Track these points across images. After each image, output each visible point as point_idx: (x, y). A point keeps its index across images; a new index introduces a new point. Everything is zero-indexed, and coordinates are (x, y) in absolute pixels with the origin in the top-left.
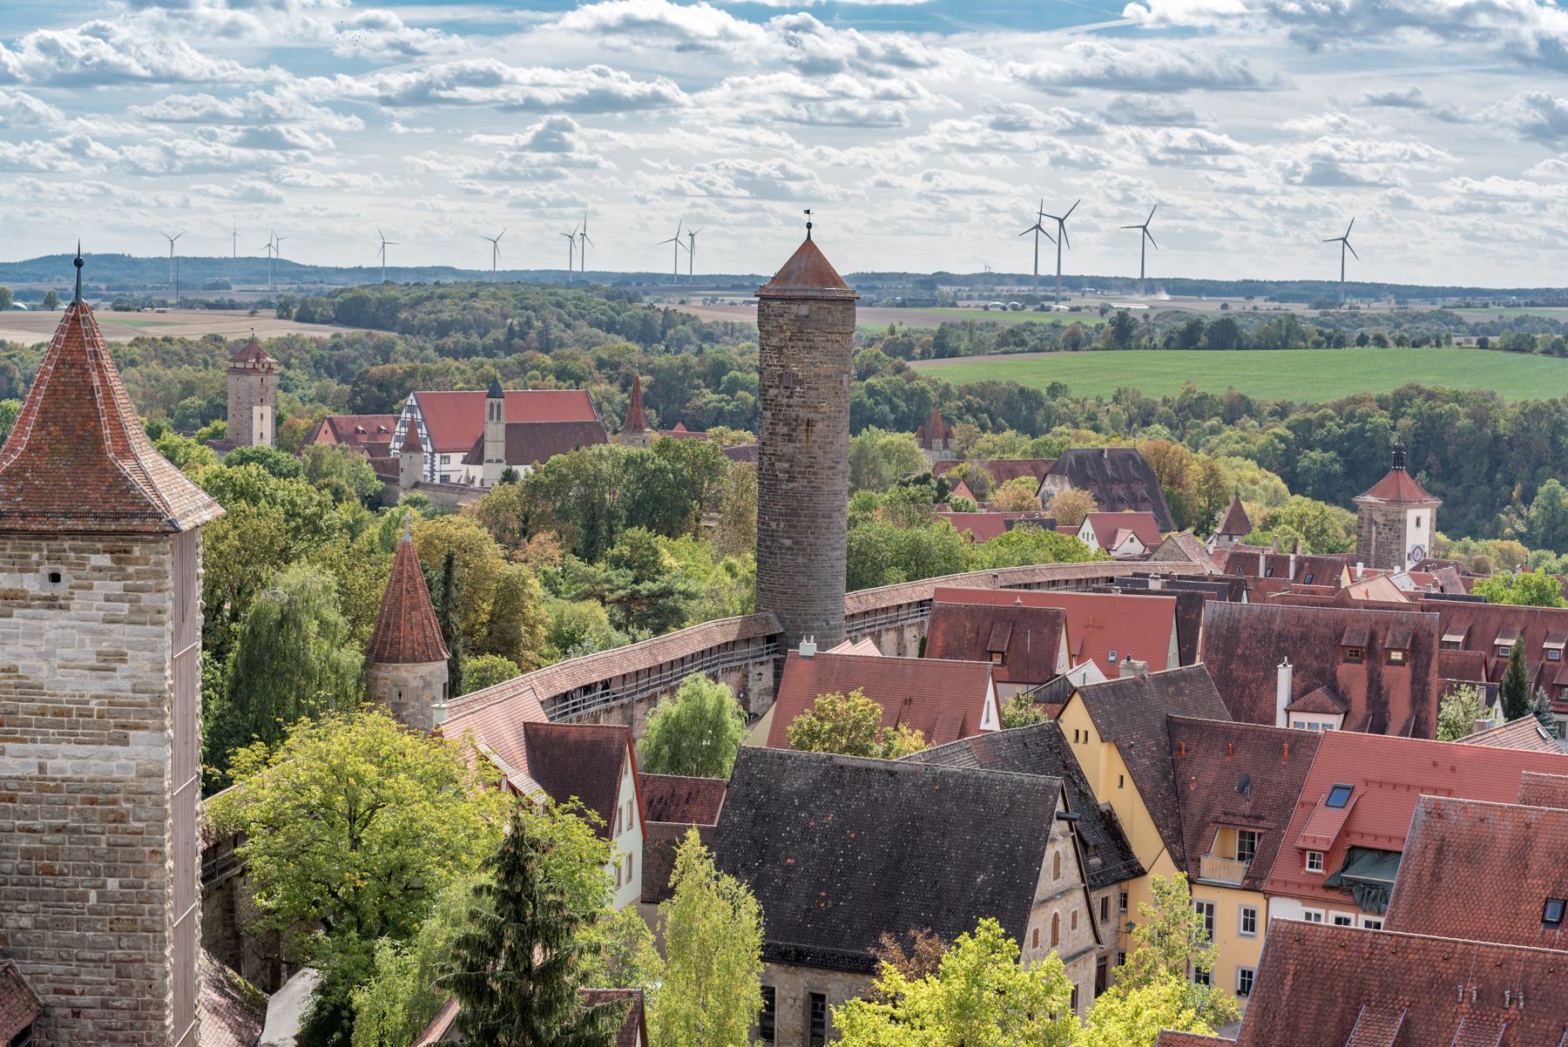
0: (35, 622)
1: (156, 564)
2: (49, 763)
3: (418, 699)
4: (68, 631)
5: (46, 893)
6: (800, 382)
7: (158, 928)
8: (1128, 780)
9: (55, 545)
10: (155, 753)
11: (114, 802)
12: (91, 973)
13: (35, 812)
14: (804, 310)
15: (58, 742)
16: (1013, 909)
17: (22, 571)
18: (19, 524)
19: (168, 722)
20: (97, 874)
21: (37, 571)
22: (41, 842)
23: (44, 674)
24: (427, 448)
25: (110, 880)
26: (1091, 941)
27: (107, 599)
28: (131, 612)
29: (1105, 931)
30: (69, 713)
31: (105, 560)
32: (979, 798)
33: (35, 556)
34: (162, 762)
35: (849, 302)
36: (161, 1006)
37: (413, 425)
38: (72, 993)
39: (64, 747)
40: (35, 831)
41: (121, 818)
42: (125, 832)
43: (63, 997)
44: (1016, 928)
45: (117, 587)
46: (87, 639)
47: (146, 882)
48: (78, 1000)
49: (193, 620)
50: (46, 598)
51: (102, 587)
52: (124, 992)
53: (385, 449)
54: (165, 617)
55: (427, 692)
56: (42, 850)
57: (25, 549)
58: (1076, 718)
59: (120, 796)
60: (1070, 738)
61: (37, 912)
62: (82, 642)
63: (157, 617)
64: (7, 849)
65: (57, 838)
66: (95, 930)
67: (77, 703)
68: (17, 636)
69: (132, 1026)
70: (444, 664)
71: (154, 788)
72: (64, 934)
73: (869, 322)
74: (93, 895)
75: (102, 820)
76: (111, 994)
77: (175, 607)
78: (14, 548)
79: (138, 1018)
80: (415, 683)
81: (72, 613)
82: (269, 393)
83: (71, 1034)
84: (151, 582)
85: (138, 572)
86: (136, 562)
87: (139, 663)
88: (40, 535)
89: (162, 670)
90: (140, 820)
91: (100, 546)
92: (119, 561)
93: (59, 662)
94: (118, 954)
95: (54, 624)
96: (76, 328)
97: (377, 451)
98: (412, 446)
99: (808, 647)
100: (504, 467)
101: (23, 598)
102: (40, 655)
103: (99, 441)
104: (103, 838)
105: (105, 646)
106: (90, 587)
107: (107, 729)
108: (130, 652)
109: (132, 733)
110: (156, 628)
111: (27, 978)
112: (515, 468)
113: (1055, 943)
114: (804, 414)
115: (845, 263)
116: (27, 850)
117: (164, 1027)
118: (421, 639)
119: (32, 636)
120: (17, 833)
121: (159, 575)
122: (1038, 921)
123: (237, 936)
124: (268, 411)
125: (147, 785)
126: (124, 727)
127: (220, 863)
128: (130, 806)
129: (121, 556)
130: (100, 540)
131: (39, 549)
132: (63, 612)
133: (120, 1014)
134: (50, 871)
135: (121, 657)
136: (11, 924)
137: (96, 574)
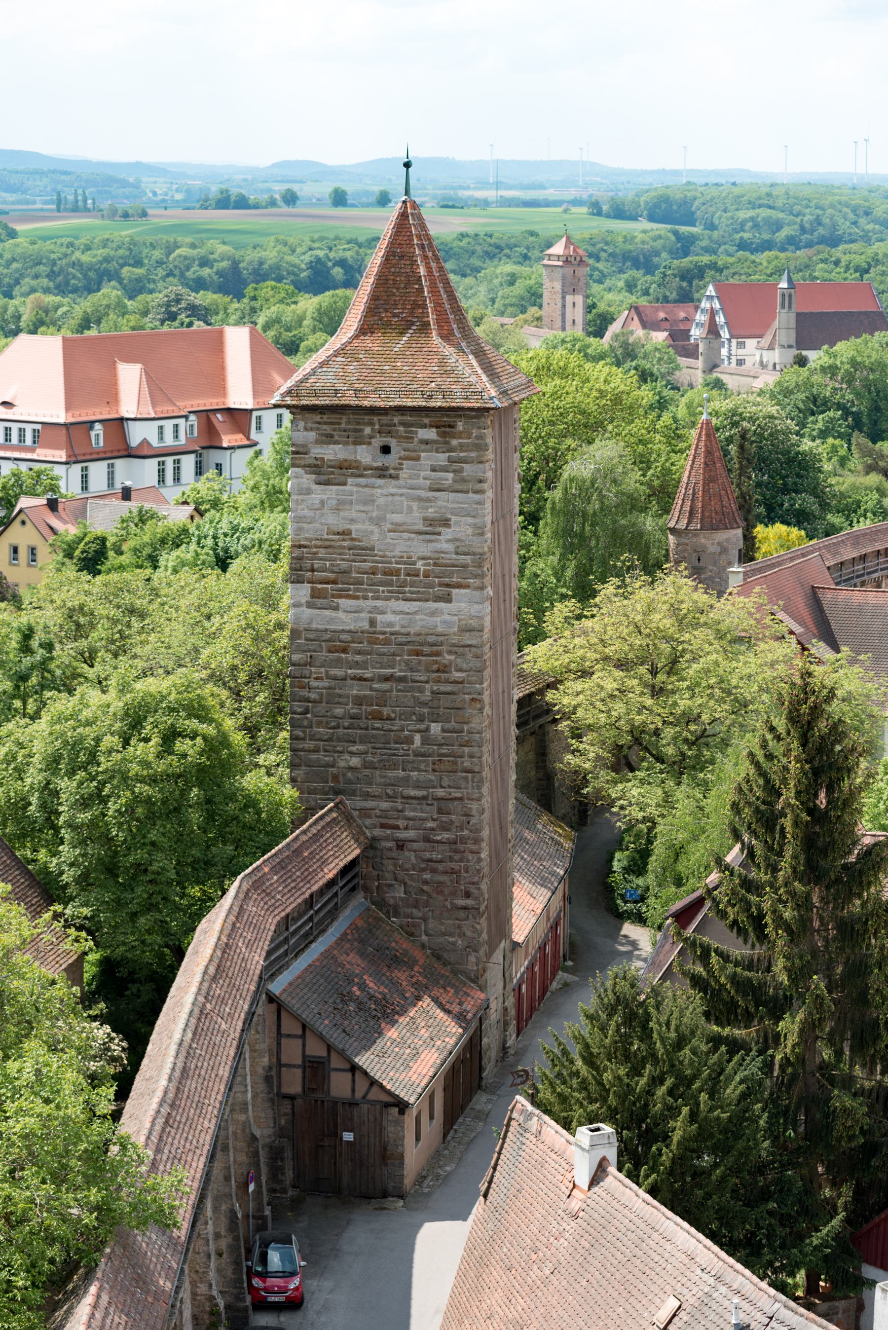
0: (367, 490)
1: (477, 437)
2: (379, 618)
3: (715, 563)
4: (397, 498)
5: (374, 736)
7: (476, 769)
9: (385, 419)
10: (475, 609)
11: (438, 654)
12: (415, 810)
13: (365, 662)
15: (388, 599)
17: (355, 443)
18: (354, 402)
19: (487, 580)
20: (421, 719)
21: (370, 443)
22: (371, 689)
23: (376, 537)
25: (433, 724)
27: (433, 470)
28: (455, 481)
30: (397, 572)
31: (431, 434)
33: (368, 430)
34: (481, 618)
36: (477, 841)
37: (713, 313)
38: (397, 827)
39: (395, 605)
40: (365, 680)
41: (444, 669)
42: (447, 681)
43: (389, 832)
45: (442, 458)
46: (415, 505)
47: (466, 727)
48: (402, 835)
49: (512, 488)
50: (377, 468)
51: (429, 458)
52: (445, 828)
53: (686, 334)
54: (485, 486)
55: (724, 557)
56: (372, 697)
57: (359, 424)
59: (444, 648)
61: (366, 753)
62: (410, 510)
63: (478, 486)
64: (340, 696)
65: (386, 686)
66: (419, 770)
67: (405, 563)
68: (351, 502)
69: (451, 859)
70: (739, 532)
71: (473, 642)
72: (391, 774)
74: (417, 738)
75: (428, 671)
76: (433, 829)
77: (495, 476)
78: (348, 423)
79: (456, 851)
80: (712, 549)
81: (401, 482)
82: (581, 284)
83: (395, 865)
84: (473, 454)
85: (461, 445)
86: (459, 435)
87: (461, 528)
88: (373, 411)
89: (482, 534)
90: (461, 670)
91: (426, 421)
92: (443, 435)
93: (389, 526)
94: (440, 793)
95: (385, 491)
96: (408, 223)
98: (713, 330)
100: (795, 352)
101: (357, 468)
102: (371, 519)
103: (425, 328)
104: (427, 686)
105: (431, 512)
106: (418, 459)
107: (431, 586)
108: (453, 518)
109: (455, 591)
110: (477, 497)
111: (355, 814)
112: (804, 353)
116: (357, 697)
117: (480, 860)
118: (718, 509)
119: (365, 503)
120: (349, 682)
121: (481, 447)
124: (579, 299)
125: (468, 639)
126: (448, 585)
128: (453, 657)
130: (427, 416)
131: (371, 424)
132: (393, 482)
133: (441, 847)
134: (378, 717)
135: (446, 523)
136: (342, 764)
137: (423, 447)
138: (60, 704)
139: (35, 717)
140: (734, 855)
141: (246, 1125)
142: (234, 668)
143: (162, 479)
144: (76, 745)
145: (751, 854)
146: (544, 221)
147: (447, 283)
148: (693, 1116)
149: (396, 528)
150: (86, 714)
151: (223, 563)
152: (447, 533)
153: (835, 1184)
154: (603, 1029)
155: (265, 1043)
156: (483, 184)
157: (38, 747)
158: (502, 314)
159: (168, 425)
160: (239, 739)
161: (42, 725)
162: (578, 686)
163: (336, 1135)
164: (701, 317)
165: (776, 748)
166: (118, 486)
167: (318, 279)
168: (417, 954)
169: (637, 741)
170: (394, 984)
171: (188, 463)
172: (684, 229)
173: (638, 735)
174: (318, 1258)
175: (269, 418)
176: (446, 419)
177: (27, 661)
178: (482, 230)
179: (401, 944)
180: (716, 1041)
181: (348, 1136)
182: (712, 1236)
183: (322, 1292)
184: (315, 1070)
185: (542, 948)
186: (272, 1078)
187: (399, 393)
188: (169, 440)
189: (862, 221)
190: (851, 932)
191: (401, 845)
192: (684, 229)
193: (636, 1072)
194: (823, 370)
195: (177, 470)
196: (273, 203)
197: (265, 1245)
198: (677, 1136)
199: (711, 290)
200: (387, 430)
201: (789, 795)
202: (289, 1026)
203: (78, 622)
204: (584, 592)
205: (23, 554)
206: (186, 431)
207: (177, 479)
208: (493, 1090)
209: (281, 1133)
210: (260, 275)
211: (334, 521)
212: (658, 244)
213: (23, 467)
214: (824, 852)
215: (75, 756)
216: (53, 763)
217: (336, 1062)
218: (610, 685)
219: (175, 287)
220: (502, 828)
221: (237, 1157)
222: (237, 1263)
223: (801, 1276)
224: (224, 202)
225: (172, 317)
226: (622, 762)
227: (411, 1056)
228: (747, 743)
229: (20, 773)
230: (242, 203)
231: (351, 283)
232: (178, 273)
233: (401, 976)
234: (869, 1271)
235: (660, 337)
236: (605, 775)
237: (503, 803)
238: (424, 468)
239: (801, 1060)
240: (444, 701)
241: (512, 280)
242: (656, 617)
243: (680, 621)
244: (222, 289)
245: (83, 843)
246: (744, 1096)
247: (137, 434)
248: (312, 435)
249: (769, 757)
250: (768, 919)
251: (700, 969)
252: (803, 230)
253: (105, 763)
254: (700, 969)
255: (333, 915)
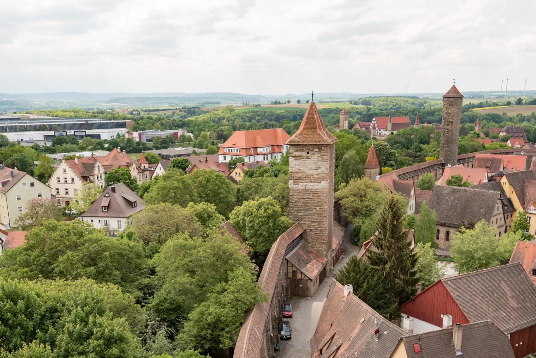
6: (450, 114)
8: (514, 192)
14: (452, 99)
16: (488, 216)
18: (302, 143)
24: (377, 128)
26: (504, 223)
29: (507, 221)
31: (317, 150)
32: (483, 195)
35: (461, 97)
37: (374, 124)
41: (320, 196)
44: (488, 220)
45: (319, 155)
58: (504, 180)
60: (502, 184)
73: (465, 102)
87: (323, 169)
88: (306, 145)
94: (319, 220)
97: (367, 129)
98: (374, 128)
99: (449, 166)
103: (316, 128)
105: (317, 166)
113: (497, 223)
114: (451, 120)
115: (461, 90)
122: (494, 219)
123: (340, 217)
124: (347, 122)
127: (337, 205)
129: (320, 149)
135: (320, 168)
138: (245, 203)
139: (241, 205)
140: (377, 233)
141: (281, 283)
142: (279, 196)
143: (264, 159)
144: (248, 211)
145: (380, 233)
146: (341, 106)
147: (320, 119)
148: (368, 283)
149: (310, 168)
150: (251, 205)
151: (276, 176)
152: (320, 170)
153: (396, 297)
154: (350, 266)
155: (285, 268)
156: (328, 98)
157: (241, 211)
158: (331, 125)
159: (265, 148)
160: (280, 210)
161: (242, 207)
162: (346, 200)
163: (298, 285)
164: (372, 125)
165: (387, 212)
166: (256, 161)
167: (294, 119)
168: (314, 251)
169: (357, 210)
170: (310, 257)
171: (269, 156)
172: (369, 106)
173: (357, 209)
174: (295, 308)
175: (285, 147)
176: (320, 147)
177: (239, 195)
178: (327, 108)
179: (311, 249)
180: (372, 269)
181: (301, 286)
182: (371, 306)
183: (295, 314)
184: (294, 273)
185: (338, 250)
186: (286, 275)
187: (310, 142)
188: (266, 152)
189: (407, 104)
190: (400, 249)
191: (311, 230)
192: (369, 106)
193: (356, 274)
194: (397, 135)
195: (267, 157)
196: (285, 103)
197: (285, 305)
198: (365, 286)
199: (374, 119)
200: (308, 149)
201: (388, 221)
202: (289, 265)
203: (248, 188)
204: (347, 182)
205: (238, 174)
206: (269, 149)
207: (267, 159)
208: (328, 277)
209: (288, 285)
210: (283, 117)
211: (297, 167)
212: (363, 110)
213: (238, 157)
214: (395, 233)
215: (248, 213)
216: (244, 215)
217: (298, 272)
218: (352, 199)
219: (266, 121)
220: (331, 228)
221: (280, 289)
222: (280, 309)
223: (388, 315)
224: (276, 103)
225: (266, 127)
226: (355, 215)
227: (312, 271)
228: (380, 211)
229: (238, 216)
230: (279, 103)
231: (301, 119)
232: (267, 118)
233: (311, 255)
234: (402, 314)
235: (364, 129)
236: (351, 217)
237: (331, 223)
238: (316, 156)
239: (390, 273)
240: (319, 203)
241: (333, 118)
242: (362, 186)
243: (366, 186)
244: (275, 121)
245: (250, 230)
246: (378, 280)
247: (260, 150)
248: (294, 150)
249: (385, 214)
250: (384, 246)
251: (369, 255)
252: (394, 106)
253: (254, 214)
254: (369, 255)
255: (298, 244)
